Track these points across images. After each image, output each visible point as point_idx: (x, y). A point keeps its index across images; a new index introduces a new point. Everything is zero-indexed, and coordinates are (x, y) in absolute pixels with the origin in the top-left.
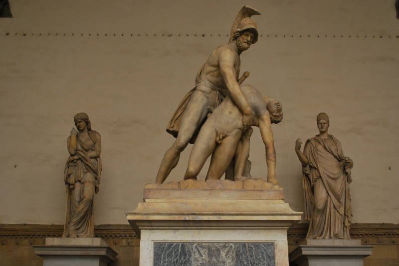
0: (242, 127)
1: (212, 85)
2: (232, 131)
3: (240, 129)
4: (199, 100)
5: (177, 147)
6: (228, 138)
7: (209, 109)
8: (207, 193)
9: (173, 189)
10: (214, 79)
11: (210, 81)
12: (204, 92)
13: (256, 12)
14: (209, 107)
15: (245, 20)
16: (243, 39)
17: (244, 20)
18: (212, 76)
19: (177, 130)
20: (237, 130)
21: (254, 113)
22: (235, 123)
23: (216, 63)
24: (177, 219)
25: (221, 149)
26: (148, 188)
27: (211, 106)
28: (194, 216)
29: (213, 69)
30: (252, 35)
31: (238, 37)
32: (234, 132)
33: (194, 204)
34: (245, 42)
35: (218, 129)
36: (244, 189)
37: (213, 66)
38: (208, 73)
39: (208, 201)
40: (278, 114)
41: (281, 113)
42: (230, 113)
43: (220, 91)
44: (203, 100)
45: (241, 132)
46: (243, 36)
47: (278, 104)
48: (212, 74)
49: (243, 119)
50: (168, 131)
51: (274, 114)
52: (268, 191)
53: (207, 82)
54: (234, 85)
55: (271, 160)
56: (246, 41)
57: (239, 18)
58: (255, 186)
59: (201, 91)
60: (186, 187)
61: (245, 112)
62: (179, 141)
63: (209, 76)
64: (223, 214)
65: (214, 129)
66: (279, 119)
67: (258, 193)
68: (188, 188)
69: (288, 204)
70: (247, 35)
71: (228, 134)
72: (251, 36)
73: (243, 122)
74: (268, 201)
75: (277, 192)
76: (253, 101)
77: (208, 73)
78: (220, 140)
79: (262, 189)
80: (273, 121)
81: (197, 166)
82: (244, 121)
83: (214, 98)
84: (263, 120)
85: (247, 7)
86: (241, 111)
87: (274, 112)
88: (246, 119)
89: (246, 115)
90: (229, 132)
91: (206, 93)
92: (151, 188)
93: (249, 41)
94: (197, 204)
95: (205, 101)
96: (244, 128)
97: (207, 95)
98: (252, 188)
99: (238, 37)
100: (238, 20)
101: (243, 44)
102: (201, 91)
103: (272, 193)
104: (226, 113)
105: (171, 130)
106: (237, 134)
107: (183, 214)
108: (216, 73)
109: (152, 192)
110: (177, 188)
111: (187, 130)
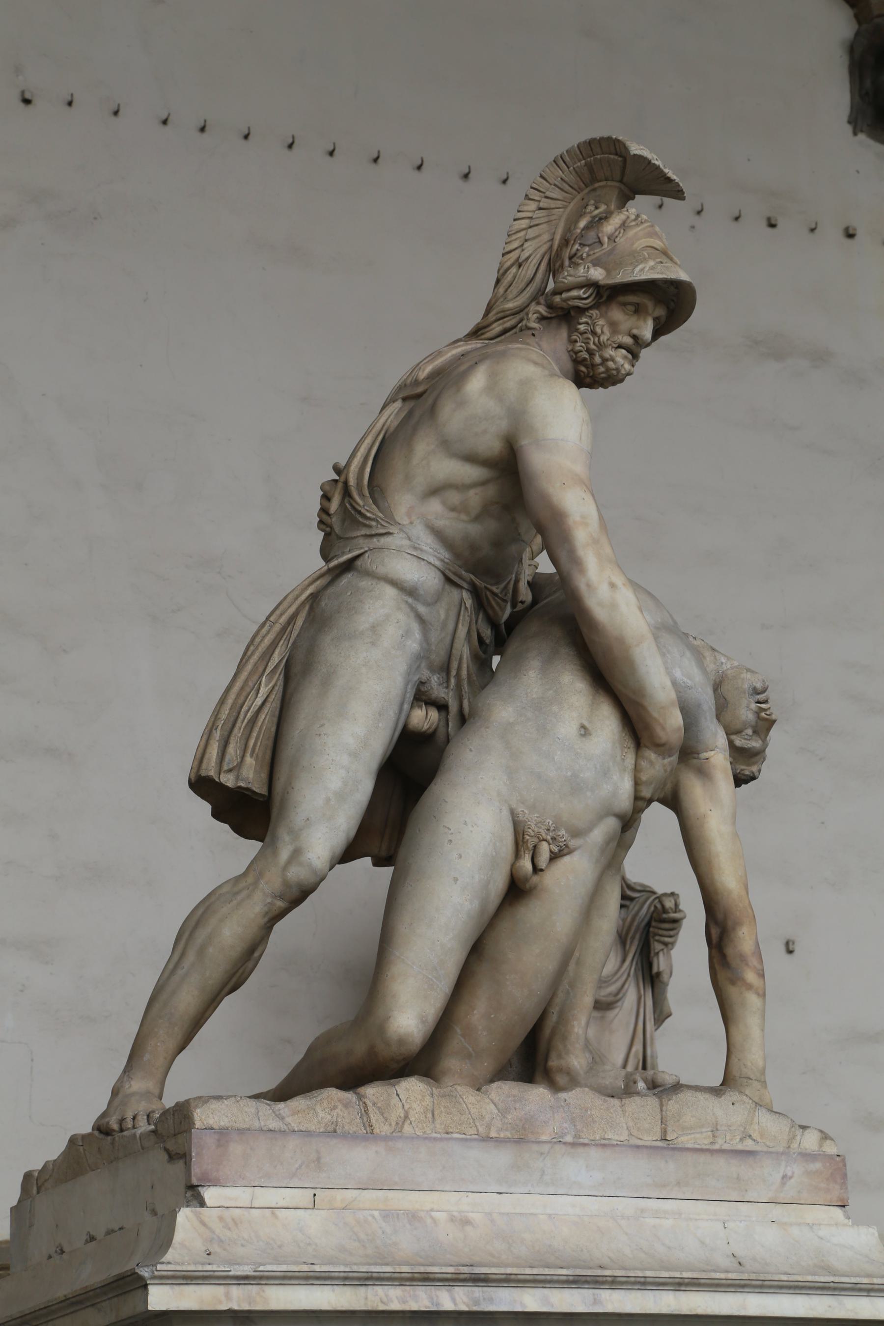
1: (446, 555)
2: (590, 829)
3: (620, 817)
4: (391, 634)
5: (286, 884)
6: (567, 859)
7: (422, 683)
8: (502, 1157)
9: (333, 1132)
10: (457, 526)
11: (438, 534)
12: (409, 591)
13: (669, 180)
14: (425, 674)
15: (624, 225)
16: (614, 326)
17: (616, 221)
18: (453, 509)
19: (259, 787)
22: (606, 789)
23: (490, 444)
24: (395, 1306)
25: (531, 913)
26: (211, 1122)
27: (432, 668)
28: (478, 1292)
29: (471, 473)
31: (581, 311)
33: (452, 1219)
34: (620, 347)
35: (520, 808)
36: (665, 1145)
37: (471, 458)
38: (435, 491)
39: (506, 1204)
40: (756, 744)
42: (585, 731)
43: (475, 592)
44: (407, 634)
46: (616, 314)
48: (454, 497)
49: (637, 769)
50: (202, 785)
51: (739, 742)
52: (777, 1156)
53: (427, 542)
54: (612, 585)
55: (749, 987)
56: (628, 340)
57: (556, 194)
58: (715, 1131)
59: (394, 583)
60: (400, 1125)
61: (662, 736)
62: (297, 853)
63: (435, 507)
64: (614, 1283)
65: (506, 813)
66: (754, 769)
67: (735, 1167)
68: (407, 1129)
69: (873, 1231)
70: (638, 310)
71: (573, 843)
72: (656, 320)
73: (637, 783)
74: (777, 1212)
75: (818, 1165)
77: (435, 491)
78: (536, 869)
79: (749, 1145)
80: (740, 780)
81: (432, 1007)
82: (644, 777)
83: (451, 626)
84: (703, 773)
85: (635, 149)
86: (636, 726)
87: (738, 732)
88: (657, 766)
89: (660, 747)
90: (576, 833)
91: (427, 604)
92: (224, 1122)
94: (466, 1222)
95: (414, 644)
97: (422, 609)
98: (702, 1139)
99: (581, 311)
100: (544, 203)
101: (609, 352)
102: (394, 583)
103: (796, 1169)
104: (567, 727)
105: (228, 780)
107: (426, 1279)
108: (475, 498)
109: (236, 1149)
110: (356, 1126)
111: (341, 796)
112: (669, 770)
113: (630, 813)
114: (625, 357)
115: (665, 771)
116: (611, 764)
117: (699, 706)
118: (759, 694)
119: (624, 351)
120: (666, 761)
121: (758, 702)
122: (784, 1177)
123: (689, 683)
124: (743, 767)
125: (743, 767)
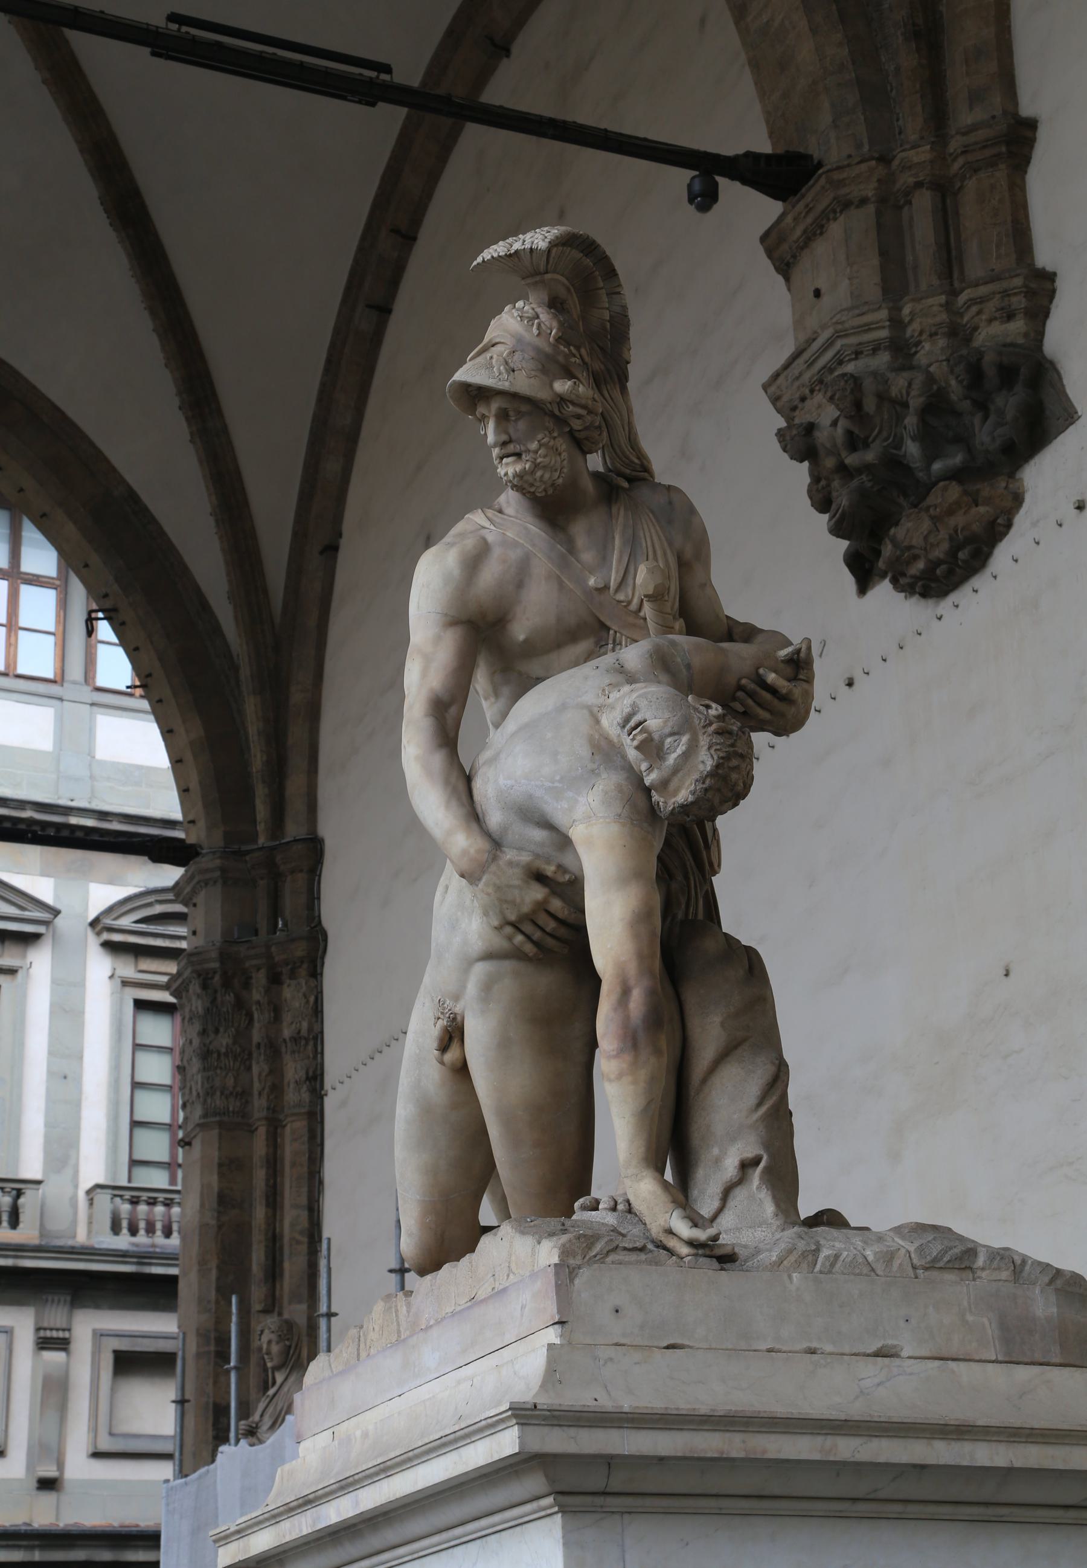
0: (498, 942)
2: (463, 987)
3: (488, 956)
20: (480, 970)
21: (538, 835)
30: (495, 406)
32: (472, 989)
34: (502, 458)
41: (671, 759)
45: (508, 965)
47: (627, 719)
71: (458, 1009)
76: (502, 781)
90: (457, 998)
93: (504, 444)
96: (510, 939)
106: (487, 987)
112: (490, 890)
113: (505, 944)
114: (507, 464)
115: (488, 894)
116: (459, 913)
117: (531, 796)
118: (624, 727)
119: (505, 460)
120: (481, 885)
121: (629, 735)
122: (523, 1307)
123: (509, 782)
124: (673, 800)
125: (673, 800)
